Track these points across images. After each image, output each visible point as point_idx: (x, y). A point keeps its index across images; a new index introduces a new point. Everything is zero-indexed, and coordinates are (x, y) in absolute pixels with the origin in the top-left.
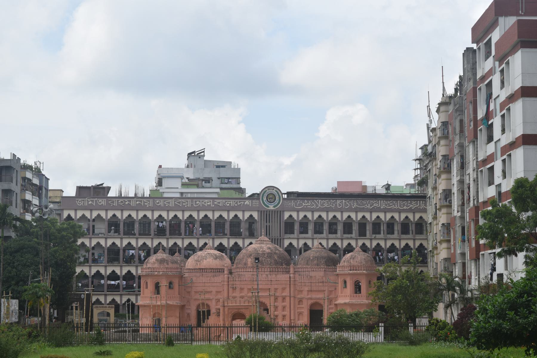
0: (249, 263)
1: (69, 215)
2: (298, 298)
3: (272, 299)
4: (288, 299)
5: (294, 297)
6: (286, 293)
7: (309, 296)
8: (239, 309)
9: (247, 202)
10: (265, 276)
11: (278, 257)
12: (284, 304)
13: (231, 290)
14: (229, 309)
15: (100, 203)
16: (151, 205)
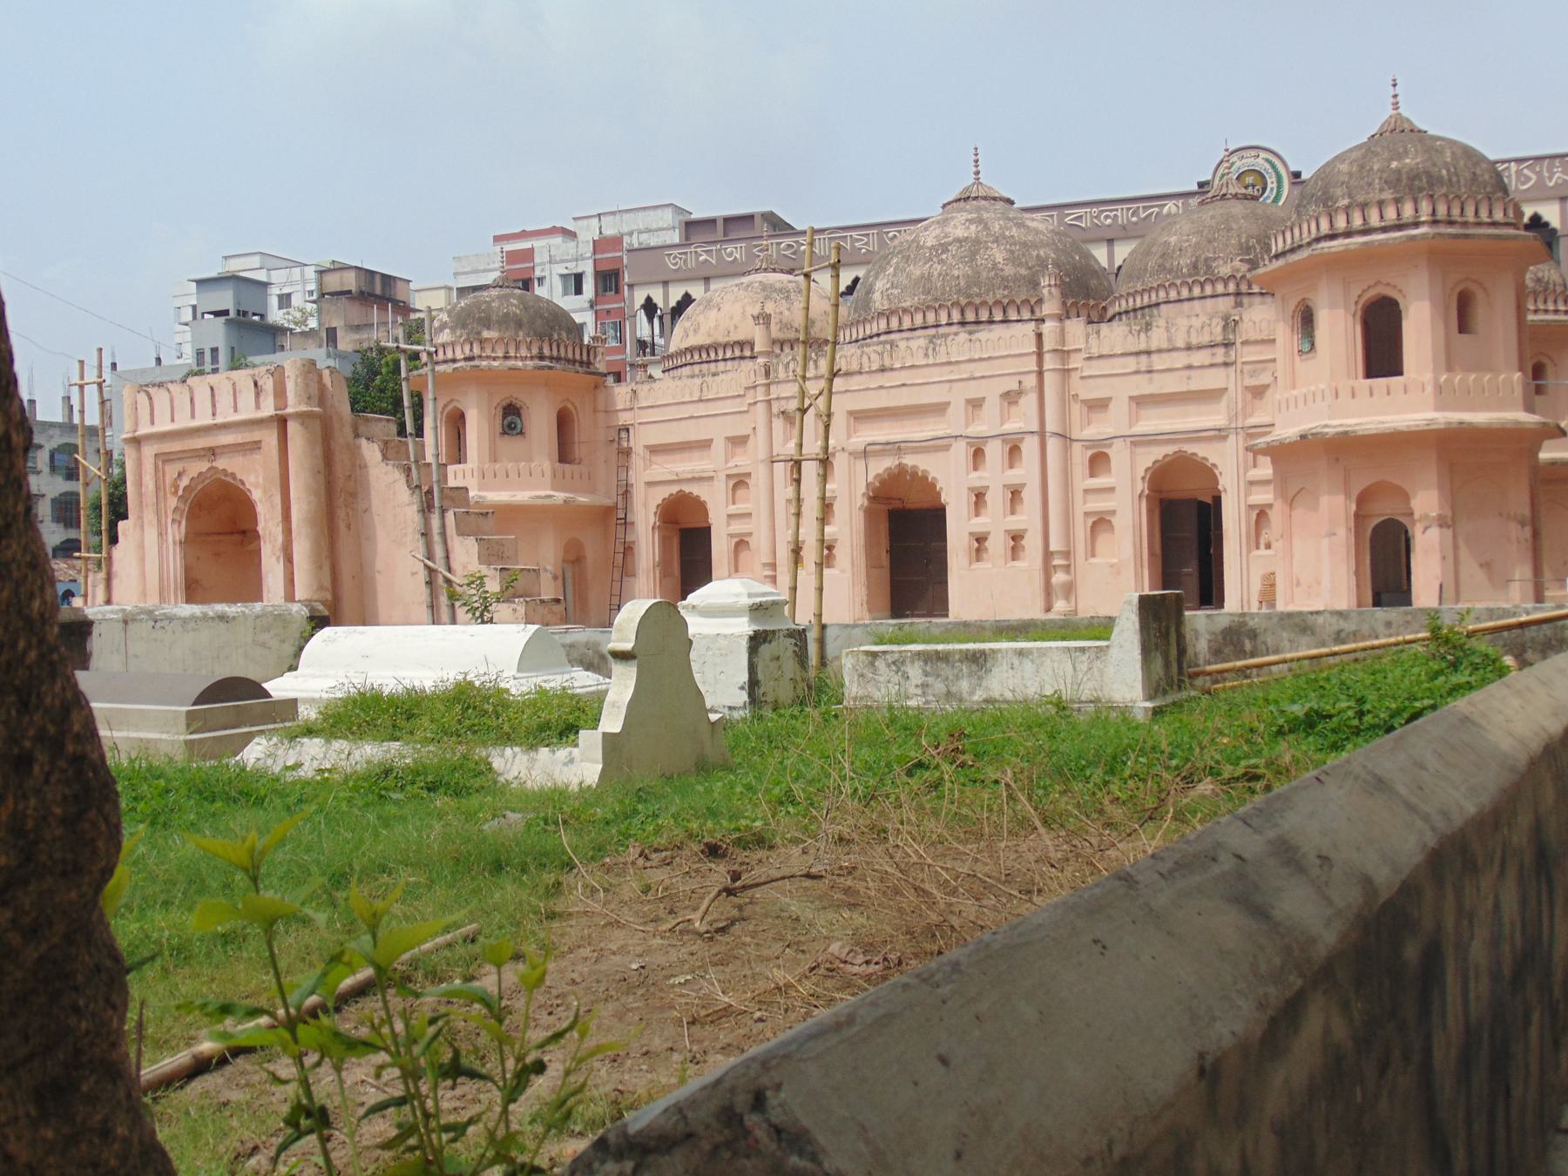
0: (877, 296)
1: (649, 299)
2: (1089, 443)
3: (961, 451)
4: (1030, 447)
5: (1065, 438)
6: (1022, 419)
7: (1143, 427)
8: (213, 452)
9: (1170, 207)
10: (922, 342)
11: (1013, 259)
12: (1015, 476)
13: (778, 424)
14: (164, 458)
15: (730, 255)
16: (874, 246)
